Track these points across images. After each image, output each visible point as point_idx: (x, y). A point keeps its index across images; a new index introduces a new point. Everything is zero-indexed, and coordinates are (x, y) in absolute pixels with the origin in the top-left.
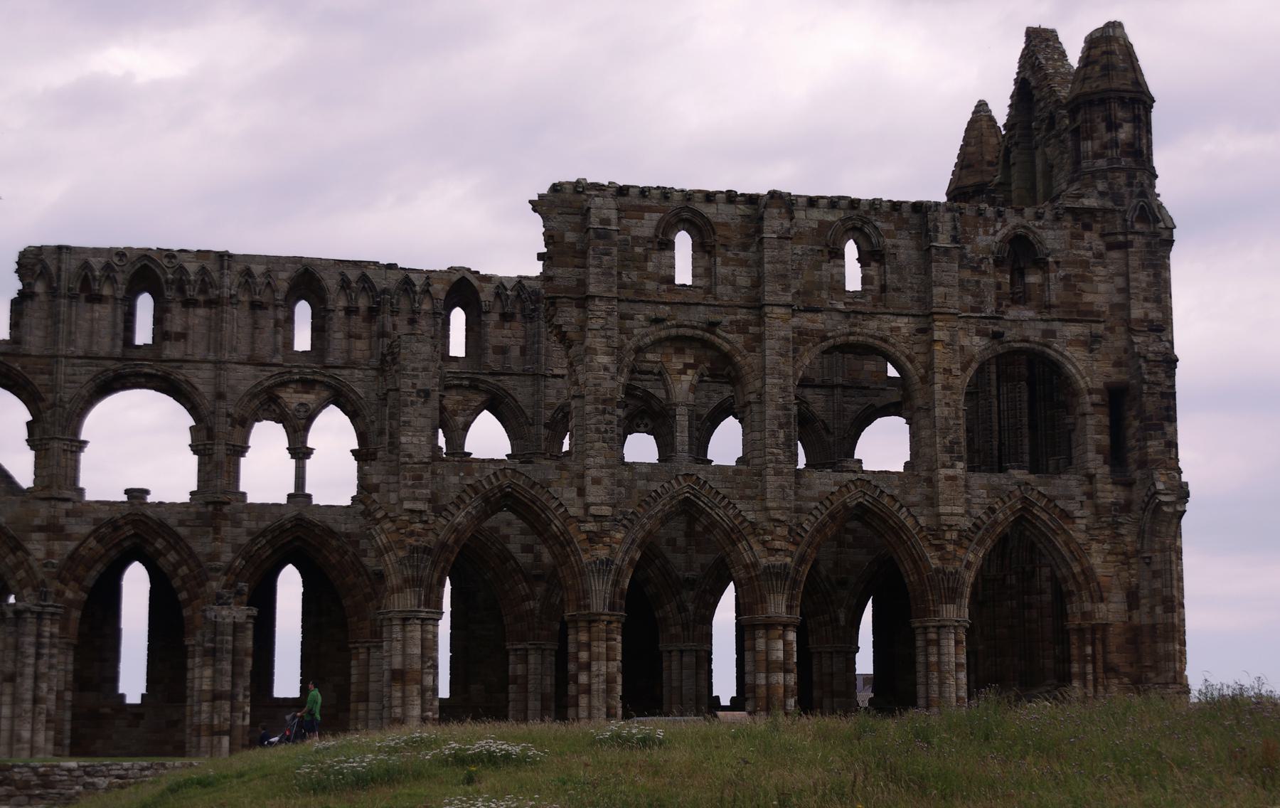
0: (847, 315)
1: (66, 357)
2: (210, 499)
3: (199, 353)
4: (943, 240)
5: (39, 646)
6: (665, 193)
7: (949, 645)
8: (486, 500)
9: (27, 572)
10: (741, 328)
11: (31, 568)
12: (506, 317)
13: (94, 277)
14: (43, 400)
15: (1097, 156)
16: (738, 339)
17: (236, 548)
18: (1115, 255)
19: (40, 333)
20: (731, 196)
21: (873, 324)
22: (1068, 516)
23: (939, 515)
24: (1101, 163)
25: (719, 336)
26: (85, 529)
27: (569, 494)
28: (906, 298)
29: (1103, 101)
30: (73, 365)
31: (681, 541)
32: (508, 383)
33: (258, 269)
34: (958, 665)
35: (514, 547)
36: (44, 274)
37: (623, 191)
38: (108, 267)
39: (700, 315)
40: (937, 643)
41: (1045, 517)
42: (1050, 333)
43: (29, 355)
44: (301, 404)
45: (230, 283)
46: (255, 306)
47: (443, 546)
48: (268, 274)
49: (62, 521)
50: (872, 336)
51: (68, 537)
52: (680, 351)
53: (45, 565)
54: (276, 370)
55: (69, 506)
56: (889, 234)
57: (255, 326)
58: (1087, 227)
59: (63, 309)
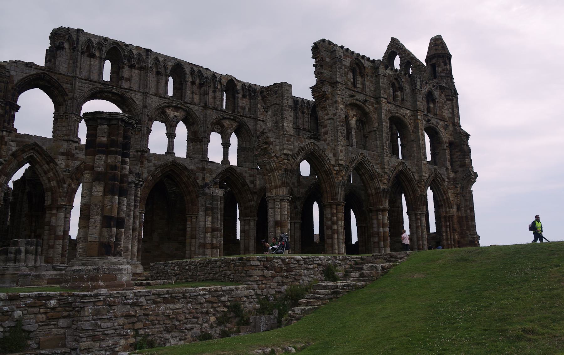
1: (79, 78)
2: (139, 150)
9: (54, 174)
11: (57, 172)
12: (244, 96)
13: (93, 47)
14: (67, 95)
15: (441, 72)
17: (149, 172)
18: (449, 102)
19: (65, 66)
23: (422, 176)
24: (443, 74)
25: (366, 106)
27: (331, 155)
28: (408, 104)
29: (443, 56)
30: (82, 83)
31: (296, 184)
32: (246, 120)
33: (161, 59)
35: (247, 181)
36: (70, 40)
38: (99, 43)
40: (420, 219)
41: (439, 180)
43: (61, 74)
44: (175, 116)
46: (158, 73)
48: (164, 62)
49: (74, 151)
50: (401, 115)
51: (76, 159)
53: (65, 171)
54: (167, 100)
55: (77, 145)
59: (79, 57)
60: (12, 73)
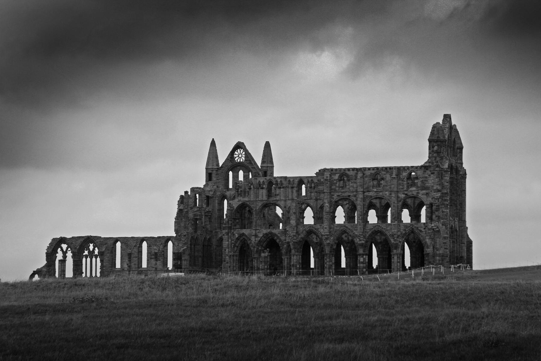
0: (376, 192)
3: (282, 198)
4: (394, 176)
5: (234, 261)
6: (340, 169)
7: (396, 257)
8: (307, 232)
10: (355, 196)
16: (354, 198)
18: (432, 175)
20: (353, 169)
21: (381, 193)
22: (421, 231)
26: (261, 235)
33: (292, 180)
34: (398, 262)
37: (332, 170)
39: (347, 194)
42: (418, 193)
45: (285, 183)
47: (300, 241)
48: (293, 181)
52: (346, 201)
56: (385, 174)
57: (292, 192)
58: (427, 169)
60: (234, 205)
